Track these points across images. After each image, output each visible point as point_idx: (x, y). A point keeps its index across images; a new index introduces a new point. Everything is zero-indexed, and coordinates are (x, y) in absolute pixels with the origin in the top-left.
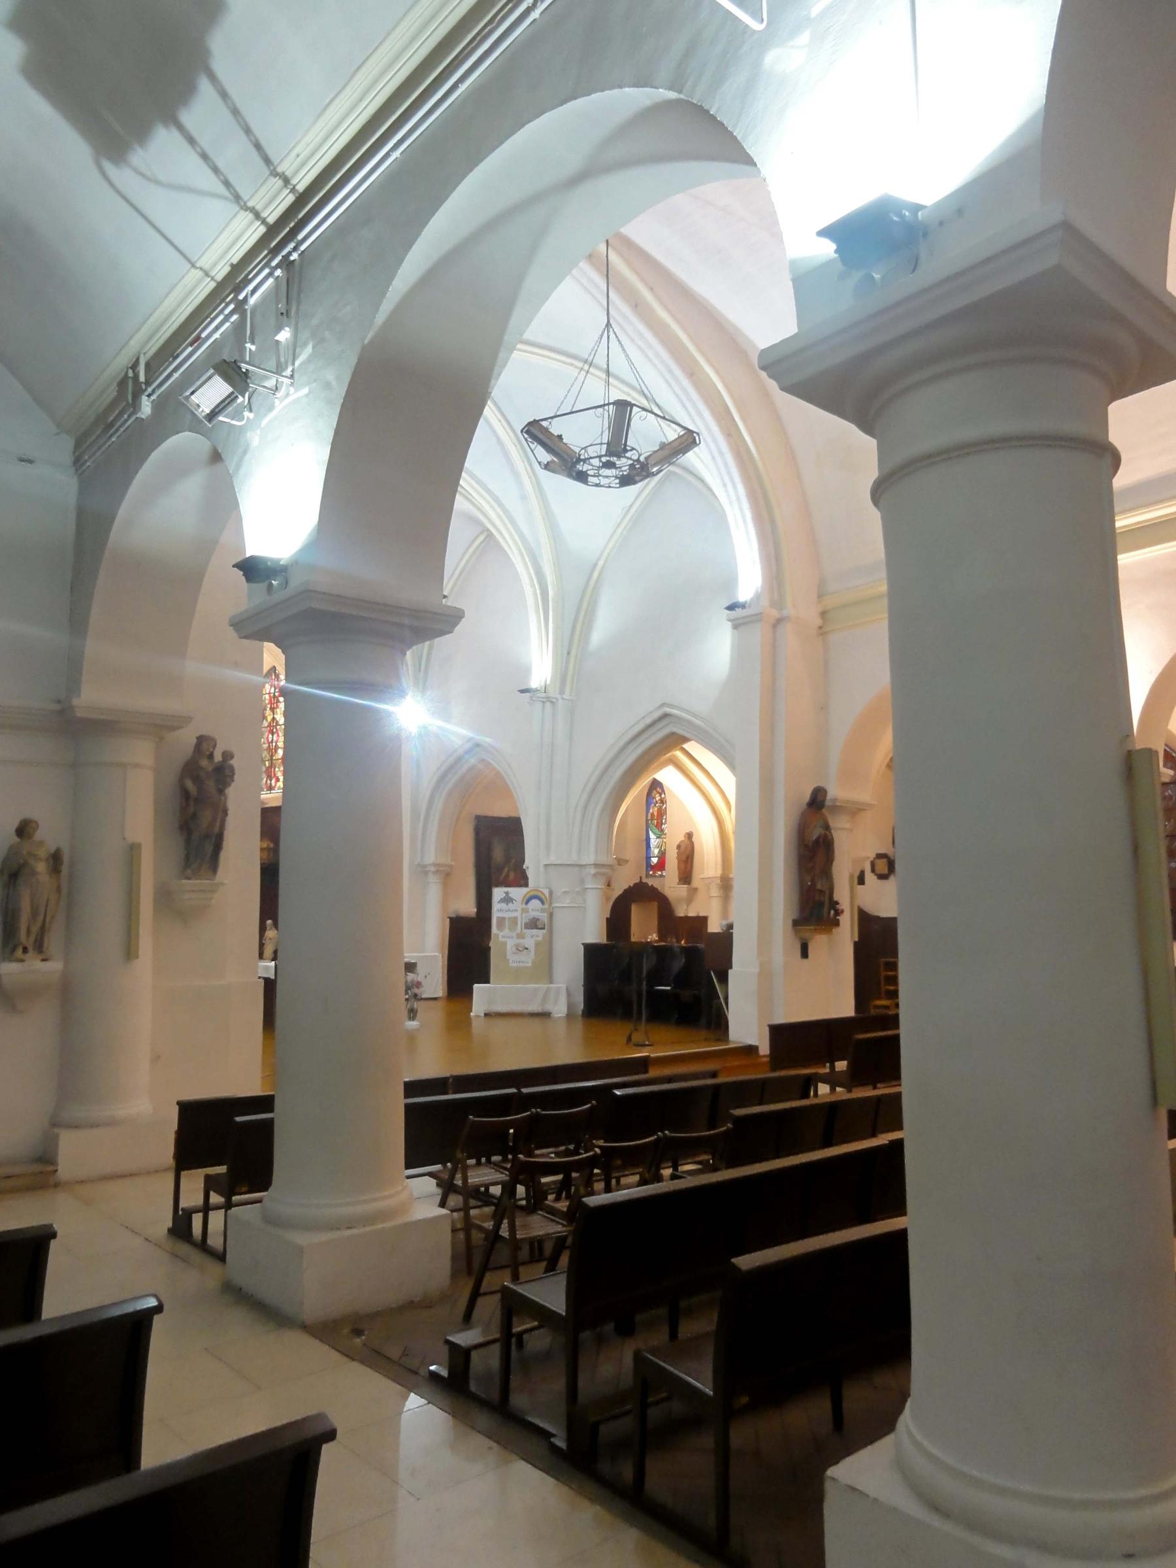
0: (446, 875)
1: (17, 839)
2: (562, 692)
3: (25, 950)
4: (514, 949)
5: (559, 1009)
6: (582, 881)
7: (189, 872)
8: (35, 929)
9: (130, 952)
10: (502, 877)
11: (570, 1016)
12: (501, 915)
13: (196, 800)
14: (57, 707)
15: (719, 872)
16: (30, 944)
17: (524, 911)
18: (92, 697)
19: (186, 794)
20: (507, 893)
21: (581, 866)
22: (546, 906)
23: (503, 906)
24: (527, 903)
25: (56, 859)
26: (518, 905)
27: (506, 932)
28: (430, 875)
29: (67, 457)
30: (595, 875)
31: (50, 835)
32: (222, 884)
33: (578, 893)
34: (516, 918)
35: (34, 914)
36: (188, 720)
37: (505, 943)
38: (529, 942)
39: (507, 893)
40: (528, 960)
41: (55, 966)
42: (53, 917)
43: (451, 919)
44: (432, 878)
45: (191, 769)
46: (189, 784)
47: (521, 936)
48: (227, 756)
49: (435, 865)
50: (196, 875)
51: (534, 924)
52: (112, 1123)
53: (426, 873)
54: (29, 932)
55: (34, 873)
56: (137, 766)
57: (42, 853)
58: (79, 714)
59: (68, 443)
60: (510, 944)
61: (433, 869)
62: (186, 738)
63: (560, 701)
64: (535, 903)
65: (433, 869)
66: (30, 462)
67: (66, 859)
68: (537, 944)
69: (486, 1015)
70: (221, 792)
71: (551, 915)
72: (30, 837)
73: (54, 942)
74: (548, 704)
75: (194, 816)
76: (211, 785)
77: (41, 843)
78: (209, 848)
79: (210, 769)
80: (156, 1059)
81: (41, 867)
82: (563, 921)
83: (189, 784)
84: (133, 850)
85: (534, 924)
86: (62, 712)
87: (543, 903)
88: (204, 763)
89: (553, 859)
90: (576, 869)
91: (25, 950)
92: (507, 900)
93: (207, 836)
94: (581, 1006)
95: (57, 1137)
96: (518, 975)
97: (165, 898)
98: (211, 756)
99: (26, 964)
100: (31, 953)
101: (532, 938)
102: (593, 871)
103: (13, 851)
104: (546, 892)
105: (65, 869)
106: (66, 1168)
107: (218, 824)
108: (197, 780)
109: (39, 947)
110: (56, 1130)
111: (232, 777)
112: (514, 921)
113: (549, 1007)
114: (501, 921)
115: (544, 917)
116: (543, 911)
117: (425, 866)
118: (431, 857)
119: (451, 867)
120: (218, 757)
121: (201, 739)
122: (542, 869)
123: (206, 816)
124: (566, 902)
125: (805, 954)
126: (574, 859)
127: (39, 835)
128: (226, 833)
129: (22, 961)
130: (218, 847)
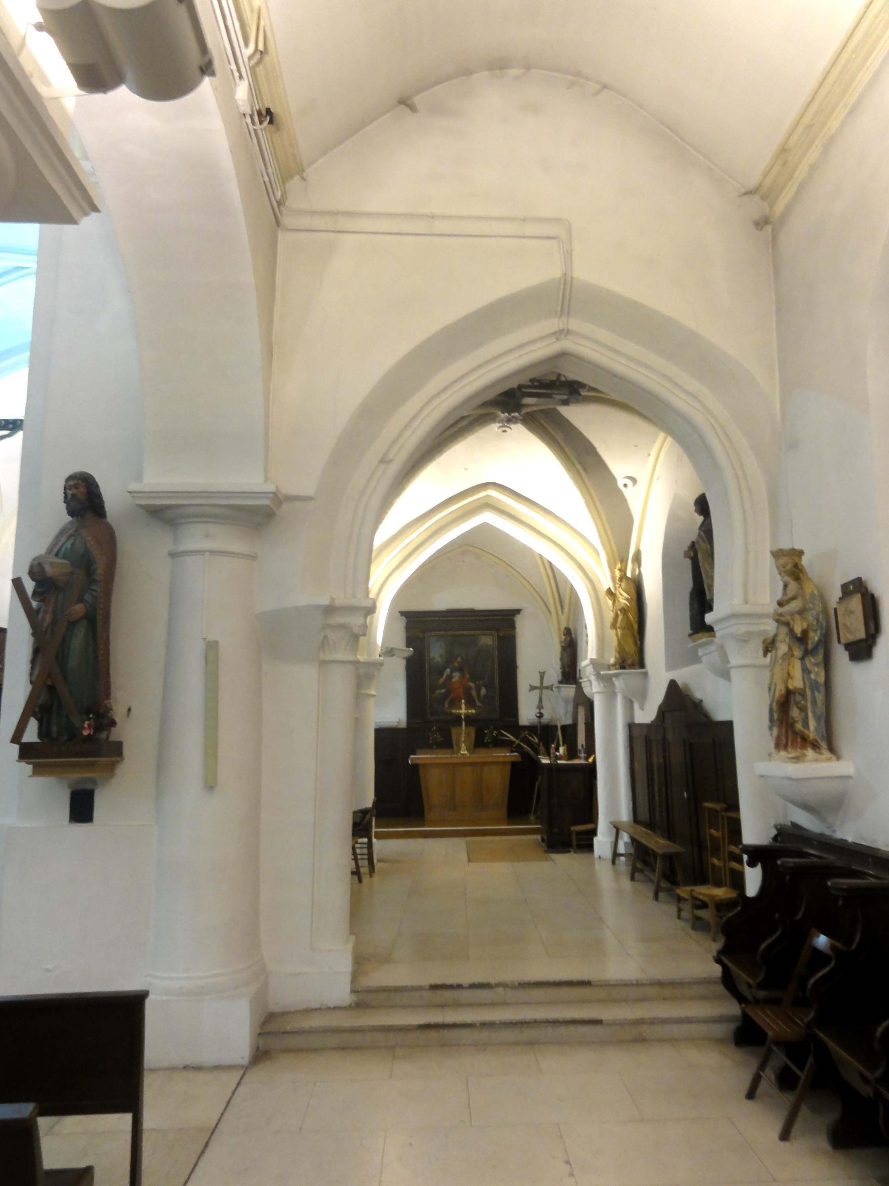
10: (441, 681)
125: (81, 809)
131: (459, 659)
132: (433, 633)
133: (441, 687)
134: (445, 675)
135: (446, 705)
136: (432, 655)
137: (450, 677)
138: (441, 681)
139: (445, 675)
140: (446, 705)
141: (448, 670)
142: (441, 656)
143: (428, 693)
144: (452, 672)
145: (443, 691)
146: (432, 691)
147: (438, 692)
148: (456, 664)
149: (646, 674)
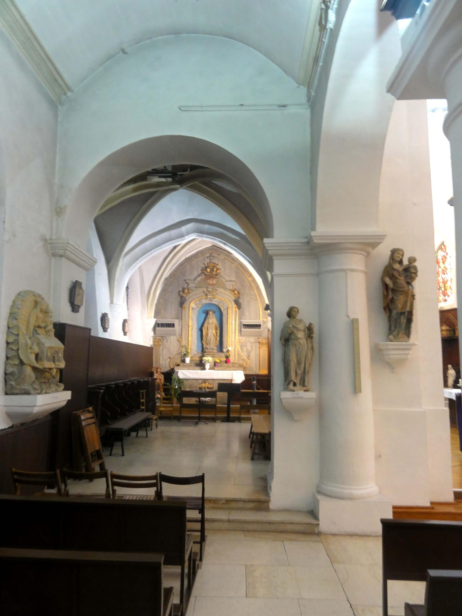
1: (288, 319)
3: (295, 384)
7: (391, 337)
8: (299, 372)
9: (356, 389)
13: (393, 290)
14: (305, 240)
16: (297, 382)
18: (324, 230)
19: (386, 286)
25: (310, 329)
29: (304, 99)
31: (307, 315)
32: (414, 345)
35: (299, 363)
36: (382, 237)
41: (312, 395)
42: (310, 365)
45: (389, 271)
46: (388, 281)
48: (412, 260)
50: (396, 338)
52: (351, 498)
54: (296, 373)
55: (297, 339)
56: (352, 270)
57: (301, 327)
58: (316, 241)
59: (304, 90)
62: (383, 253)
66: (284, 106)
67: (316, 329)
70: (409, 283)
72: (294, 318)
73: (312, 379)
75: (392, 300)
76: (402, 280)
77: (301, 321)
78: (403, 320)
79: (401, 269)
80: (378, 457)
81: (301, 335)
83: (388, 281)
84: (354, 323)
86: (308, 243)
88: (397, 266)
91: (295, 384)
93: (402, 313)
95: (318, 501)
97: (377, 354)
98: (401, 262)
99: (295, 393)
100: (298, 386)
103: (286, 326)
105: (315, 335)
106: (325, 524)
107: (408, 304)
108: (392, 277)
109: (303, 383)
110: (319, 497)
111: (416, 273)
120: (406, 262)
121: (394, 252)
123: (400, 301)
127: (299, 317)
128: (414, 312)
129: (294, 391)
130: (409, 320)
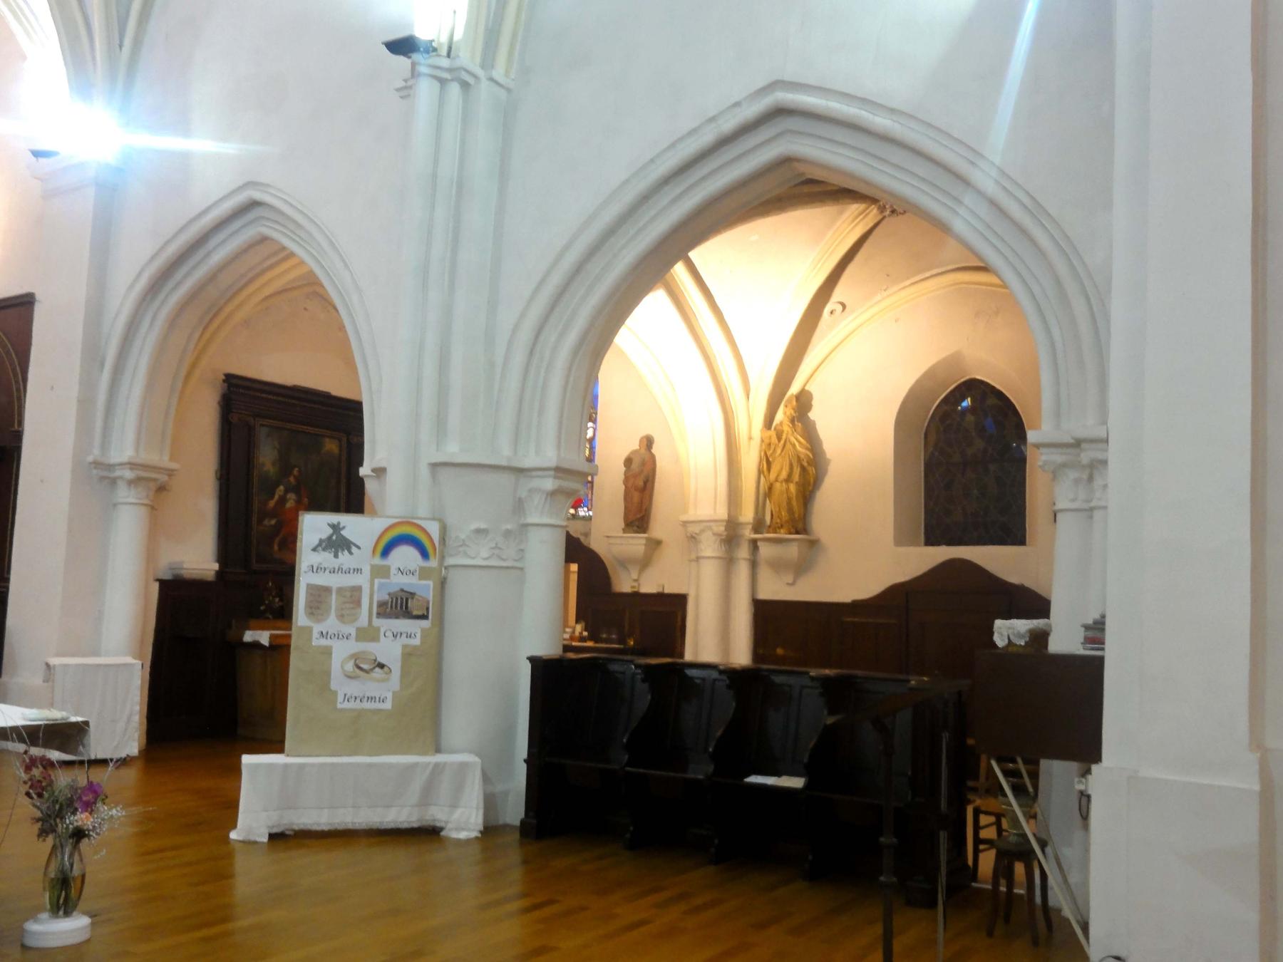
0: (158, 488)
2: (488, 60)
4: (350, 667)
5: (463, 820)
6: (519, 506)
10: (272, 503)
11: (490, 831)
12: (321, 580)
15: (722, 513)
17: (380, 572)
20: (336, 528)
21: (520, 471)
22: (433, 563)
23: (326, 558)
24: (386, 552)
26: (363, 557)
27: (331, 623)
28: (122, 486)
30: (553, 494)
33: (507, 534)
34: (358, 589)
37: (327, 652)
38: (389, 649)
39: (336, 528)
40: (383, 692)
43: (164, 584)
44: (124, 494)
47: (368, 634)
49: (132, 465)
51: (400, 606)
53: (113, 482)
60: (341, 652)
61: (129, 474)
63: (484, 90)
64: (405, 556)
65: (129, 474)
68: (408, 654)
69: (273, 837)
71: (442, 584)
74: (454, 89)
82: (469, 601)
85: (400, 606)
87: (425, 554)
89: (453, 450)
90: (506, 479)
92: (337, 543)
94: (514, 811)
96: (357, 731)
101: (394, 642)
102: (549, 484)
104: (434, 529)
112: (353, 596)
113: (437, 814)
114: (319, 596)
115: (426, 589)
116: (424, 573)
117: (111, 467)
118: (124, 449)
119: (171, 473)
122: (424, 472)
124: (481, 553)
126: (504, 454)
131: (296, 471)
132: (266, 422)
133: (273, 514)
134: (276, 497)
135: (276, 548)
136: (261, 460)
137: (283, 500)
138: (272, 503)
139: (276, 497)
140: (276, 548)
141: (282, 488)
142: (274, 464)
143: (255, 519)
144: (287, 491)
145: (273, 522)
146: (260, 521)
147: (266, 522)
148: (292, 479)
149: (814, 544)
